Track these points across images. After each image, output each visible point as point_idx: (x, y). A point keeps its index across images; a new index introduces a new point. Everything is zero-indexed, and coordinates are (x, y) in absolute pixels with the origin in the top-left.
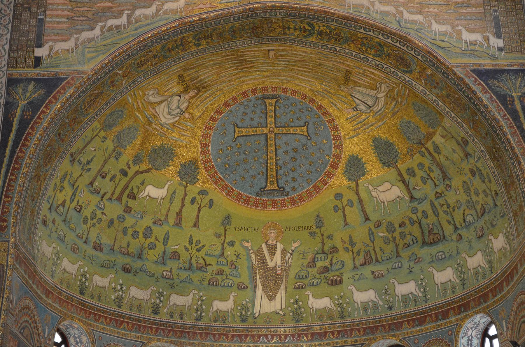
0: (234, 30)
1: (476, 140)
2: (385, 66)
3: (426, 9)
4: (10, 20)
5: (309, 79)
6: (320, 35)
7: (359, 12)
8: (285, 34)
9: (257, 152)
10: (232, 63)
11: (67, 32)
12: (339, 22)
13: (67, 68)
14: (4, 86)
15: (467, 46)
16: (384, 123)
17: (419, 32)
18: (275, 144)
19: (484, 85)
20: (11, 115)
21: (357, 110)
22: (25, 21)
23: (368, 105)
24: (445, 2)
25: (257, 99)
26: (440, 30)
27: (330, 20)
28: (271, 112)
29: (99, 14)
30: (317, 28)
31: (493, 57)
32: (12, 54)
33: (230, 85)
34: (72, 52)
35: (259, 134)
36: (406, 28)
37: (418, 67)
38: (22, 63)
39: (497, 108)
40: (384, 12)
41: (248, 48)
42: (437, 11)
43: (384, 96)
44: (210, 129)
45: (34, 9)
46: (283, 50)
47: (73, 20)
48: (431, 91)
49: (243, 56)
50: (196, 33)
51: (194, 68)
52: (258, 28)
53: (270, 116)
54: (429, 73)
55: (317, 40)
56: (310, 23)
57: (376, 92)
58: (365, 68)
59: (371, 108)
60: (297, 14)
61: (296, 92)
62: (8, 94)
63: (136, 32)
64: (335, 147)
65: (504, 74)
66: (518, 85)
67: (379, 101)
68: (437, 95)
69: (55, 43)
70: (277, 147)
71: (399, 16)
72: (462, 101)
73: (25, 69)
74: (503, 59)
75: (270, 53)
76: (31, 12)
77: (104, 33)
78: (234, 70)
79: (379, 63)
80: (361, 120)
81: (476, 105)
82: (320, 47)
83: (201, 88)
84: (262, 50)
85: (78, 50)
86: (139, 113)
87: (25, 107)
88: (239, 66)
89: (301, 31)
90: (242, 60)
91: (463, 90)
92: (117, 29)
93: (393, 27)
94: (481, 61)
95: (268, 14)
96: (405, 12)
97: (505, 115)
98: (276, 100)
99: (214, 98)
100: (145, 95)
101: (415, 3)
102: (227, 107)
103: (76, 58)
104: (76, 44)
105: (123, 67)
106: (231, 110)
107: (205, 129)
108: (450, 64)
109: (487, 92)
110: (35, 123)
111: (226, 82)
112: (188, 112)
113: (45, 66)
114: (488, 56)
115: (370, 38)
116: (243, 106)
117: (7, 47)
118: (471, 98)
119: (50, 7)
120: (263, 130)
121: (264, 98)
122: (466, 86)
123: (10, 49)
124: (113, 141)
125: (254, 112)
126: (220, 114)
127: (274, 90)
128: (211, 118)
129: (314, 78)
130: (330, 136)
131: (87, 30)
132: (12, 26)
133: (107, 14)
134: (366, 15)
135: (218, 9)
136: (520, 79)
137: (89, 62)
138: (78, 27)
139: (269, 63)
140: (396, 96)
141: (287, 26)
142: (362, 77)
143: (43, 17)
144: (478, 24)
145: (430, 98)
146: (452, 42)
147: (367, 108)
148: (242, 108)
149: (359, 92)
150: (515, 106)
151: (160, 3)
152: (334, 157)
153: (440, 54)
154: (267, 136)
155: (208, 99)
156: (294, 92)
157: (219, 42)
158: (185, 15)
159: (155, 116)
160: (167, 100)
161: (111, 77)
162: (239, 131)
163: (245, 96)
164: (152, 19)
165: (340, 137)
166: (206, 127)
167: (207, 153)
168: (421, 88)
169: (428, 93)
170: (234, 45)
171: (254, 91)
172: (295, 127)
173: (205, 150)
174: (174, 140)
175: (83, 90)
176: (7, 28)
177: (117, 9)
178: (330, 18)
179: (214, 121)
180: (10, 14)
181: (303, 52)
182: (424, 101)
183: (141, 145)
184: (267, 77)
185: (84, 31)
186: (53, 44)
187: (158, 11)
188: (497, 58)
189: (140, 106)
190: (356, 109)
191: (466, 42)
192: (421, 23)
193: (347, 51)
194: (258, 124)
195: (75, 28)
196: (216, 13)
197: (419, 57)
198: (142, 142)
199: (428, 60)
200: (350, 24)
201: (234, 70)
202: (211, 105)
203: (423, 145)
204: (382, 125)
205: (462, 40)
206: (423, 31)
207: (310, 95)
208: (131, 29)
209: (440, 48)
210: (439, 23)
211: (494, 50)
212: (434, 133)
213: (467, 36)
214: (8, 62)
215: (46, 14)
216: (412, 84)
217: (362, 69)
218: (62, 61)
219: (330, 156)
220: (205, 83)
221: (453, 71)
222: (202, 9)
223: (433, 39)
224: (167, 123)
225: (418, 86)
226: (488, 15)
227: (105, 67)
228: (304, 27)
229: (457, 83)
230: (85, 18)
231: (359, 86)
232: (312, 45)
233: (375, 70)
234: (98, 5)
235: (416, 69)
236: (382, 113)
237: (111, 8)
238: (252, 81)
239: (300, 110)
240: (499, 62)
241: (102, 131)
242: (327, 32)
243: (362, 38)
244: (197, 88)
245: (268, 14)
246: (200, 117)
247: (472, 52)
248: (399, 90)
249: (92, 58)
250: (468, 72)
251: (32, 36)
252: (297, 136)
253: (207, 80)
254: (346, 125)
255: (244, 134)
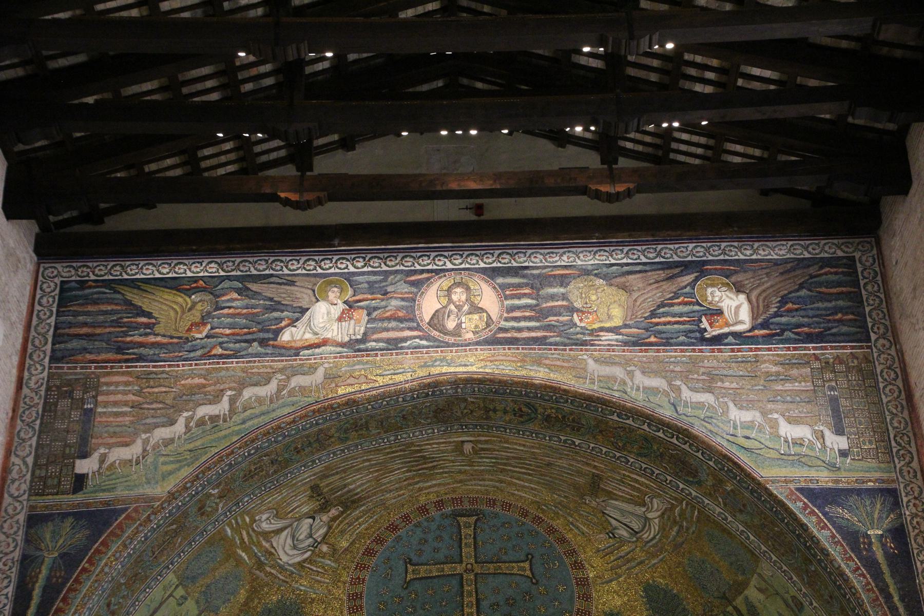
0: (404, 415)
1: (815, 604)
2: (657, 472)
3: (719, 384)
4: (38, 413)
5: (532, 486)
6: (546, 421)
7: (609, 388)
8: (488, 418)
9: (445, 606)
10: (402, 463)
11: (130, 430)
12: (576, 404)
13: (127, 492)
14: (22, 528)
15: (789, 446)
16: (661, 560)
17: (709, 423)
18: (476, 592)
19: (820, 515)
20: (30, 579)
21: (615, 537)
22: (63, 414)
23: (632, 529)
24: (749, 372)
25: (444, 516)
26: (743, 420)
27: (562, 401)
28: (468, 537)
29: (184, 397)
30: (540, 410)
31: (832, 467)
32: (38, 472)
33: (399, 496)
34: (137, 463)
35: (449, 575)
36: (687, 416)
37: (710, 477)
38: (54, 487)
39: (844, 555)
40: (649, 389)
41: (427, 440)
42: (737, 386)
43: (659, 517)
44: (364, 568)
45: (78, 394)
46: (486, 442)
47: (141, 408)
48: (734, 516)
49: (419, 451)
50: (342, 423)
51: (337, 473)
52: (444, 410)
53: (466, 544)
54: (729, 489)
55: (542, 428)
56: (529, 404)
57: (644, 509)
58: (624, 472)
59: (638, 535)
60: (508, 391)
61: (510, 505)
62: (27, 541)
63: (244, 426)
64: (579, 598)
65: (851, 496)
66: (876, 516)
67: (650, 525)
68: (745, 524)
69: (110, 449)
70: (480, 596)
71: (674, 396)
72: (786, 537)
73: (57, 497)
74: (850, 470)
75: (465, 446)
76: (72, 399)
77: (190, 430)
78: (404, 472)
79: (646, 466)
80: (622, 554)
81: (809, 548)
82: (547, 438)
83: (350, 503)
84: (450, 442)
85: (146, 461)
86: (243, 552)
87: (54, 563)
88: (413, 466)
89: (515, 415)
90: (419, 457)
91: (786, 521)
92: (211, 423)
93: (666, 413)
94: (813, 473)
95: (459, 390)
96: (684, 388)
97: (858, 568)
98: (475, 518)
99: (371, 518)
100: (255, 521)
101: (701, 373)
102: (392, 532)
103: (143, 473)
104: (144, 450)
105: (220, 484)
106: (400, 536)
107: (356, 569)
108: (762, 477)
109: (825, 527)
110: (70, 590)
111: (391, 491)
112: (327, 543)
113: (91, 490)
114: (825, 465)
115: (629, 428)
116: (420, 529)
117: (30, 460)
118: (799, 536)
119: (105, 388)
120: (455, 568)
121: (456, 515)
122: (790, 515)
123: (35, 464)
124: (197, 602)
125: (439, 538)
126: (381, 543)
127: (473, 503)
128: (366, 550)
129: (539, 483)
130: (570, 578)
131: (163, 426)
132: (41, 424)
133: (197, 396)
134: (620, 393)
135: (378, 385)
136: (878, 506)
137: (164, 479)
138: (148, 421)
139: (463, 461)
140: (678, 518)
141: (491, 407)
142: (620, 485)
143: (92, 406)
144: (805, 410)
145: (734, 526)
146: (762, 440)
147: (631, 534)
148: (419, 531)
149: (615, 508)
150: (874, 553)
151: (284, 377)
152: (578, 614)
153: (744, 459)
154: (462, 577)
155: (360, 520)
156: (507, 506)
157: (379, 433)
158: (324, 397)
159: (271, 554)
160: (291, 525)
161: (200, 500)
162: (413, 571)
163: (423, 512)
164: (271, 403)
165: (587, 580)
166: (357, 566)
167: (357, 611)
168: (718, 510)
169: (730, 519)
170: (404, 436)
171: (439, 504)
172: (511, 562)
173: (355, 605)
174: (301, 591)
175: (153, 527)
176: (33, 428)
177: (213, 387)
178: (561, 397)
179: (371, 556)
180: (38, 404)
181: (520, 445)
182: (724, 530)
183: (246, 604)
184: (461, 481)
185: (158, 427)
186: (107, 451)
187: (279, 390)
188: (839, 469)
189: (246, 540)
190: (613, 534)
191: (786, 441)
192: (710, 407)
193: (593, 445)
194: (446, 557)
195: (144, 422)
196: (374, 392)
197: (711, 463)
198: (247, 598)
199: (726, 469)
200: (594, 406)
201: (404, 472)
202: (366, 529)
203: (729, 601)
204: (658, 562)
205: (780, 437)
206: (715, 421)
207: (533, 511)
208: (236, 422)
209: (743, 450)
210: (741, 408)
211: (833, 455)
212: (744, 585)
213: (787, 430)
214: (31, 486)
215: (96, 401)
216: (703, 502)
217: (619, 473)
218: (121, 480)
219: (572, 612)
220: (357, 494)
221: (766, 489)
222: (352, 385)
223: (732, 435)
224: (290, 562)
225: (712, 506)
226: (821, 395)
227: (190, 487)
228: (520, 409)
229: (774, 509)
230: (161, 406)
231: (616, 500)
232: (534, 435)
233: (641, 476)
234: (183, 382)
235: (707, 481)
236: (657, 543)
237: (204, 386)
238: (435, 489)
239: (517, 535)
240: (844, 474)
241: (180, 587)
242: (557, 417)
243: (616, 428)
244: (342, 503)
245: (459, 390)
246: (347, 549)
247: (797, 457)
248: (682, 509)
249: (170, 473)
250: (792, 491)
251: (73, 439)
252: (513, 577)
253: (359, 490)
254: (597, 561)
255: (422, 575)
